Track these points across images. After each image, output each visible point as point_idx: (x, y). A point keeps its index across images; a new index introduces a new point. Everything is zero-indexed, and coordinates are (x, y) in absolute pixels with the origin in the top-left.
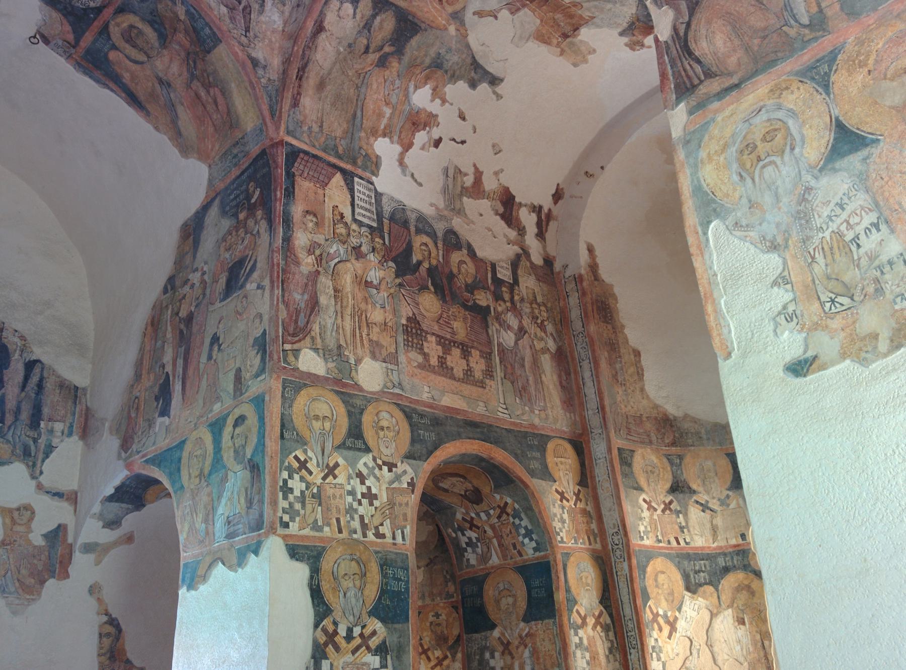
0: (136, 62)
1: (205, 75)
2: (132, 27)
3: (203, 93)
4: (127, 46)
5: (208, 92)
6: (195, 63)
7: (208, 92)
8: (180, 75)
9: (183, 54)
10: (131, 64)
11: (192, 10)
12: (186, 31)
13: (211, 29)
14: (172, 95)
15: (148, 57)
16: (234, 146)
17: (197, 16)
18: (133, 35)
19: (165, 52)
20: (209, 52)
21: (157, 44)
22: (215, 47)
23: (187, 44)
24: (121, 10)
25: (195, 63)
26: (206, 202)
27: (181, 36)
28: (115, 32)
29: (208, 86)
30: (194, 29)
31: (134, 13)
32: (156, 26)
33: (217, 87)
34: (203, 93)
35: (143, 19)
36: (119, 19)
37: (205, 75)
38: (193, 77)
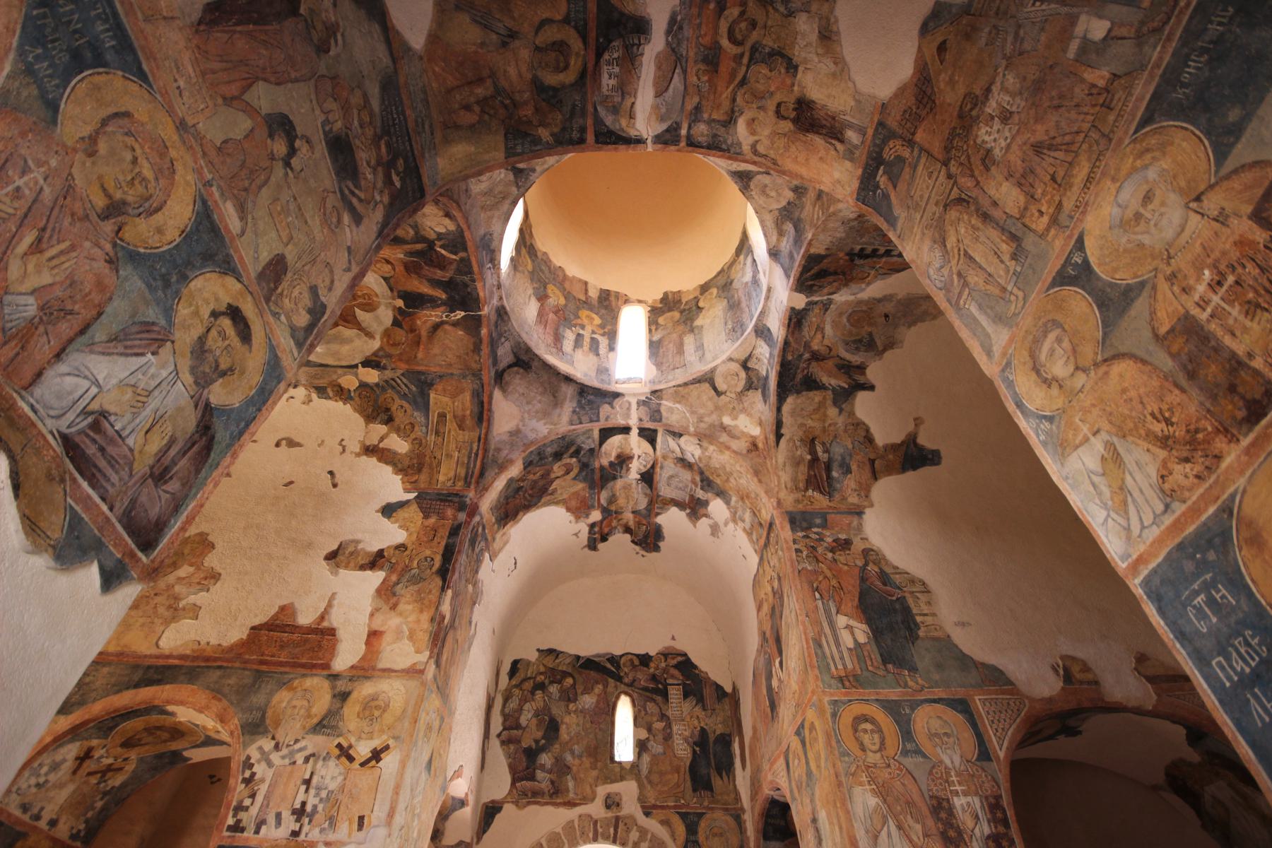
0: (544, 23)
1: (492, 112)
2: (566, 67)
3: (480, 91)
4: (558, 37)
5: (478, 102)
6: (506, 107)
7: (478, 102)
8: (505, 71)
9: (517, 97)
10: (544, 16)
11: (539, 147)
12: (529, 122)
13: (519, 154)
14: (494, 36)
15: (538, 49)
16: (431, 126)
17: (533, 148)
18: (562, 58)
19: (529, 76)
20: (505, 135)
21: (539, 74)
22: (506, 148)
23: (522, 113)
24: (583, 75)
25: (506, 107)
26: (389, 25)
27: (528, 112)
28: (576, 44)
29: (483, 102)
30: (526, 135)
31: (572, 85)
32: (551, 93)
33: (479, 122)
34: (480, 91)
35: (563, 86)
36: (580, 63)
37: (492, 112)
38: (498, 91)
